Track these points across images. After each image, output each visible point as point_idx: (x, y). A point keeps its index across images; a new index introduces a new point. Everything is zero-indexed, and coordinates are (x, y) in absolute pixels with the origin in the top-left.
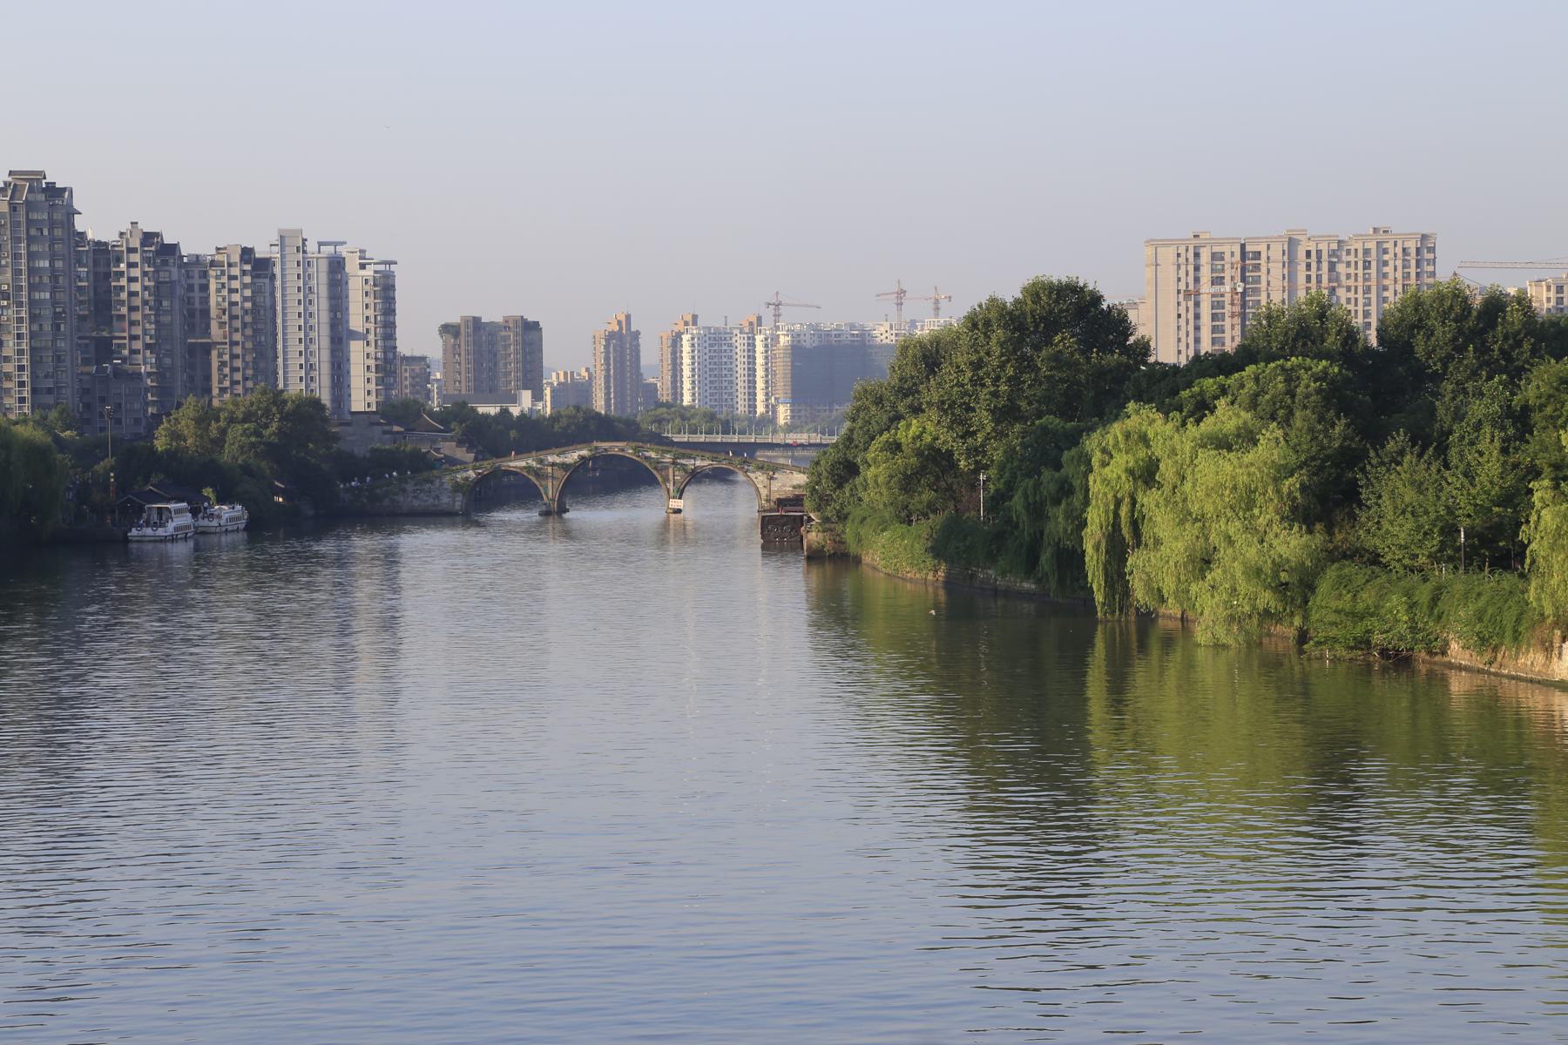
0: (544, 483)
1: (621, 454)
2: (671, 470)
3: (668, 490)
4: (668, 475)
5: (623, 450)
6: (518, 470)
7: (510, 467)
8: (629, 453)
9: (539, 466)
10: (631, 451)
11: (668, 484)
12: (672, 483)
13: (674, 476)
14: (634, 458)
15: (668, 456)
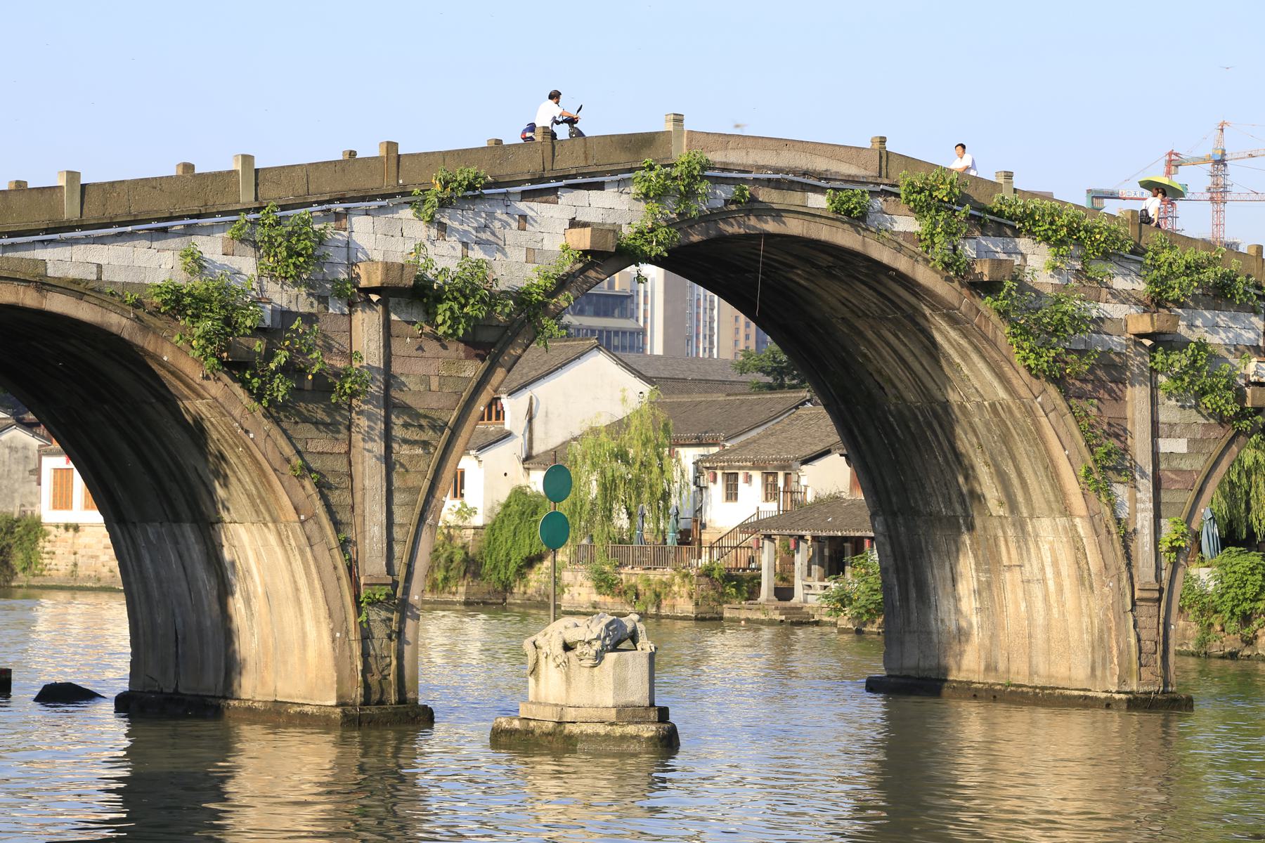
0: (319, 443)
1: (845, 237)
2: (1137, 397)
3: (1127, 538)
4: (1118, 432)
5: (857, 218)
6: (116, 321)
7: (44, 285)
8: (898, 243)
9: (281, 296)
10: (906, 224)
11: (1121, 491)
12: (1146, 485)
13: (1155, 434)
14: (925, 275)
15: (1119, 283)
